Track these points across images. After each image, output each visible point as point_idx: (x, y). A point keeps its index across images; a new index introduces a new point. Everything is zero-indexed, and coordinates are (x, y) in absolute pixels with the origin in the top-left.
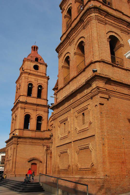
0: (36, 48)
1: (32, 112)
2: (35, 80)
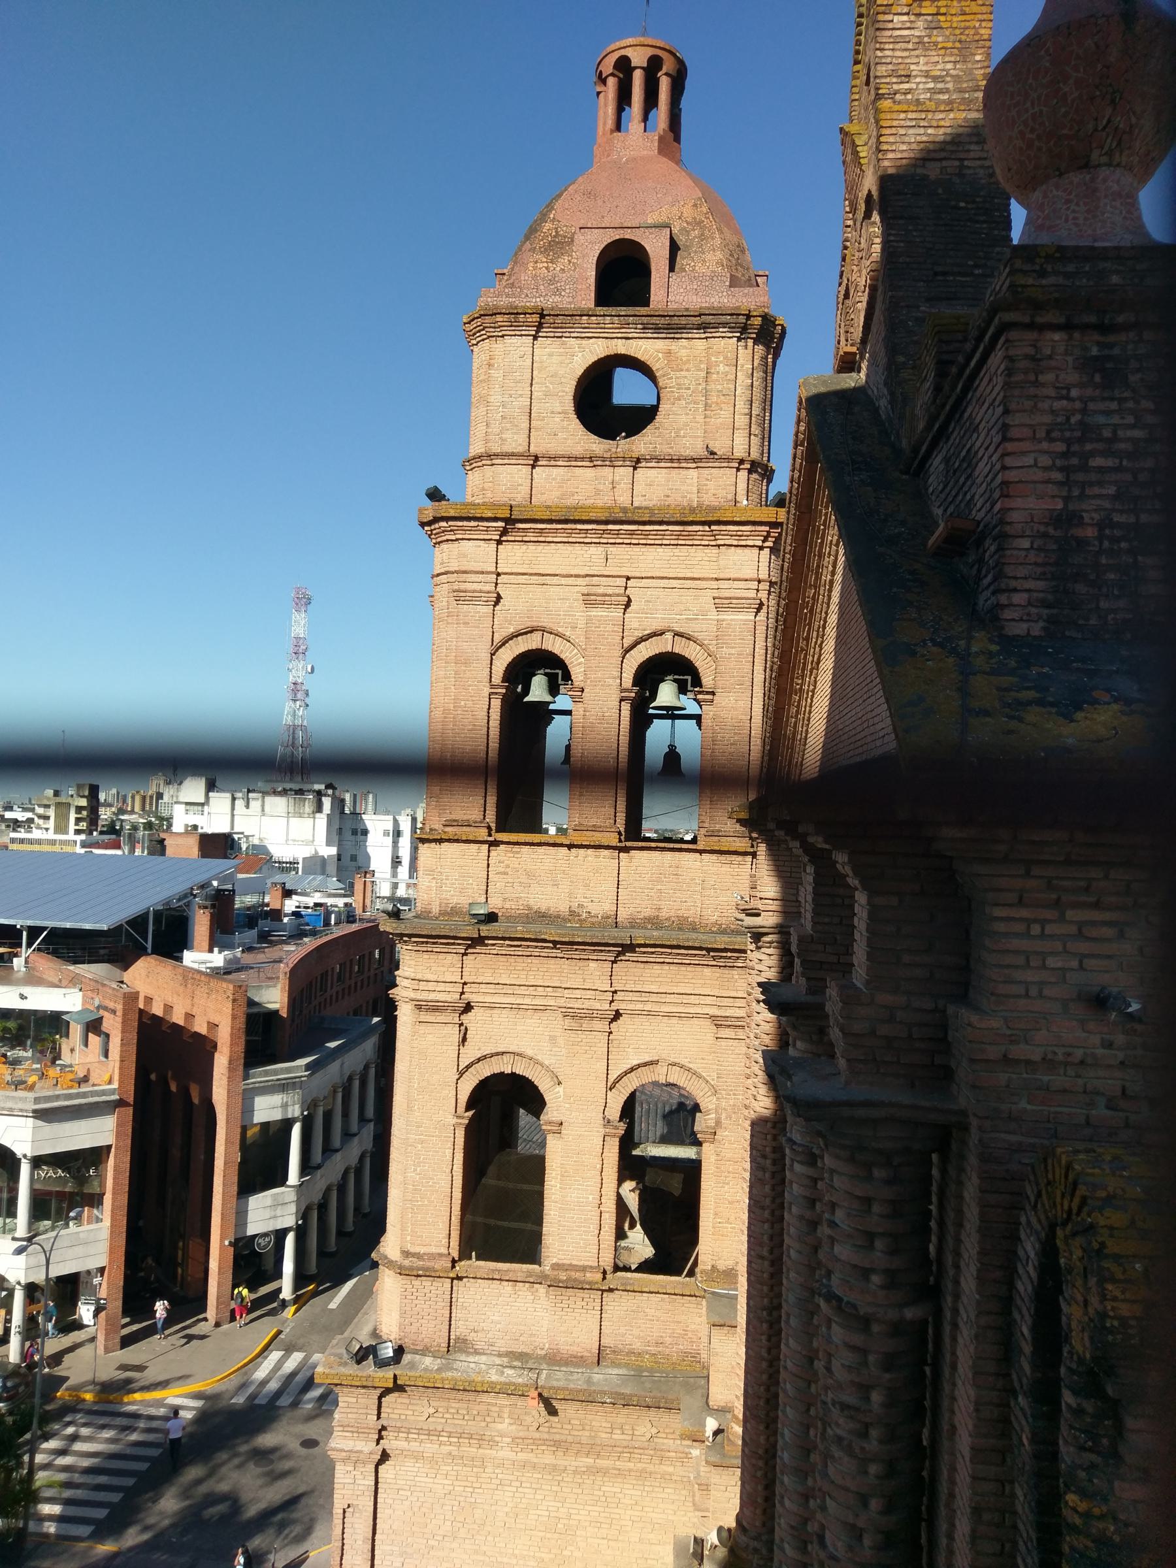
0: (638, 78)
1: (553, 1039)
2: (589, 600)
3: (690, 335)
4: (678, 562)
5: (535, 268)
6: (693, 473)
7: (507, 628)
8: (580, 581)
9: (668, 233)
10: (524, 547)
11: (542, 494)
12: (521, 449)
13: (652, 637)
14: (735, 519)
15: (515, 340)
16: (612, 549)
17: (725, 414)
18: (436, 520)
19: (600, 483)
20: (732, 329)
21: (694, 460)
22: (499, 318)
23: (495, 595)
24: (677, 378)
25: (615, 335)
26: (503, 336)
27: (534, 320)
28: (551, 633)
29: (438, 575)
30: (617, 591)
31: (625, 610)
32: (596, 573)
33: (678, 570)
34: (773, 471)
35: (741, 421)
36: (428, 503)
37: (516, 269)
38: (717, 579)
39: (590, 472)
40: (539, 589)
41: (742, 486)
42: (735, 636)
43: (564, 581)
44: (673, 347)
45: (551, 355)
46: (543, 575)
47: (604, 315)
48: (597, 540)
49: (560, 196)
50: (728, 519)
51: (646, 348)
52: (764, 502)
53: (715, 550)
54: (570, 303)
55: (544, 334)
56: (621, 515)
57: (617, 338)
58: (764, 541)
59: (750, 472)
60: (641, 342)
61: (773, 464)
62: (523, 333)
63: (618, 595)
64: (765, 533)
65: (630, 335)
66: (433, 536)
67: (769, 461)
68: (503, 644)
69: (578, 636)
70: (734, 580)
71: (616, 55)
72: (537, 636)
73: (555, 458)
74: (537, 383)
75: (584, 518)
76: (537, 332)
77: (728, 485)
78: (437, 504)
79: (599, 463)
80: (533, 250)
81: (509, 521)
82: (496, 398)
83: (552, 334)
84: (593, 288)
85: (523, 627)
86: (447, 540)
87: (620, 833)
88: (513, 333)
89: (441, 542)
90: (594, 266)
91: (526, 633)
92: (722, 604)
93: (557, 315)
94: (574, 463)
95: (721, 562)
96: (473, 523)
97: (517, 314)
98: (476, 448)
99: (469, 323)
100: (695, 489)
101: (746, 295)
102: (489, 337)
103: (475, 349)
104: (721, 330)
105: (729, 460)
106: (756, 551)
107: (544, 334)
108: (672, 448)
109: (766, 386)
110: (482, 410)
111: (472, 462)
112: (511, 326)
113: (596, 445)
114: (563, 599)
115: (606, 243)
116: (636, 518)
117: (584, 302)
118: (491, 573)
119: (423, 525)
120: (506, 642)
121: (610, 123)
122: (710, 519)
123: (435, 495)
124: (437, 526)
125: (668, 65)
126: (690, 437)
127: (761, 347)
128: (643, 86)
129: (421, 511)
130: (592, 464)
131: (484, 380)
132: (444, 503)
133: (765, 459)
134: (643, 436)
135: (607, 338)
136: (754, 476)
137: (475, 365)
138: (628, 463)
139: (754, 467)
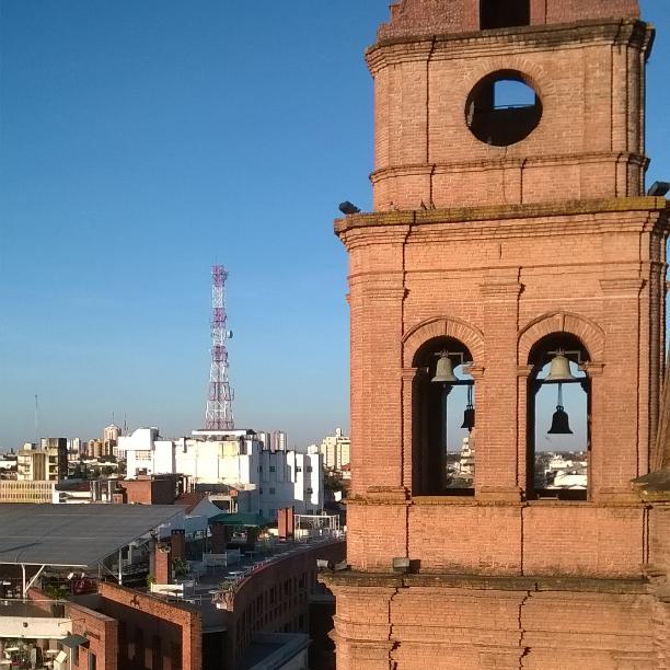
2: (485, 289)
8: (477, 274)
12: (419, 161)
15: (411, 65)
17: (603, 115)
20: (606, 36)
21: (575, 157)
22: (396, 47)
30: (510, 281)
34: (649, 161)
35: (619, 119)
36: (342, 215)
39: (482, 177)
40: (442, 283)
41: (621, 179)
47: (490, 36)
51: (528, 59)
53: (599, 239)
54: (458, 28)
60: (523, 57)
61: (648, 155)
63: (512, 284)
73: (451, 166)
76: (430, 56)
82: (396, 118)
83: (443, 57)
87: (522, 493)
92: (607, 285)
96: (381, 229)
98: (383, 163)
105: (609, 155)
113: (486, 150)
118: (399, 272)
119: (338, 233)
129: (337, 221)
131: (386, 103)
132: (356, 214)
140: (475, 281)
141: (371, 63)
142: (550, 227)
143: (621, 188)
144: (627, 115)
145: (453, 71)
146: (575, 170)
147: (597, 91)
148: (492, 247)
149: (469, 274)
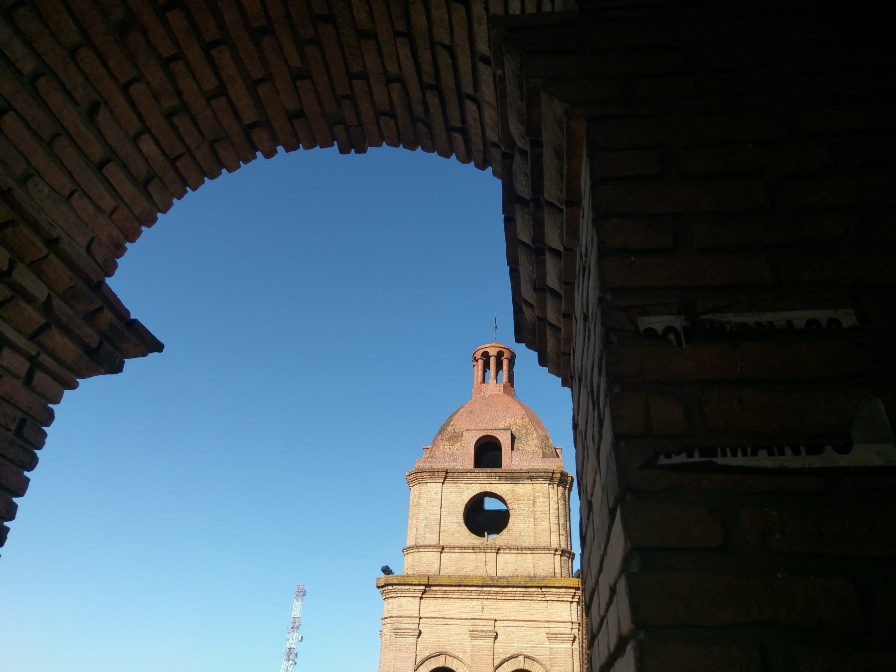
0: (493, 361)
2: (474, 634)
3: (524, 482)
4: (524, 610)
5: (443, 448)
6: (530, 556)
7: (425, 653)
8: (468, 622)
9: (510, 432)
10: (436, 601)
11: (446, 568)
12: (435, 543)
13: (511, 659)
14: (555, 585)
16: (486, 602)
17: (545, 524)
18: (386, 585)
19: (478, 562)
20: (545, 479)
22: (425, 474)
23: (418, 631)
24: (518, 504)
25: (484, 482)
26: (427, 483)
27: (443, 475)
28: (451, 656)
29: (385, 618)
31: (495, 641)
32: (477, 617)
33: (525, 615)
35: (554, 527)
36: (382, 575)
37: (434, 448)
38: (548, 622)
39: (473, 556)
40: (444, 627)
41: (558, 564)
42: (561, 658)
43: (458, 622)
44: (515, 488)
45: (451, 492)
46: (446, 619)
47: (479, 472)
48: (477, 597)
49: (456, 413)
50: (551, 585)
51: (501, 488)
52: (571, 575)
53: (545, 603)
54: (461, 466)
55: (448, 482)
56: (490, 582)
57: (485, 483)
58: (573, 598)
59: (561, 556)
60: (498, 486)
61: (574, 551)
62: (437, 481)
63: (490, 631)
64: (573, 594)
65: (492, 482)
66: (384, 594)
67: (571, 549)
68: (422, 664)
69: (467, 658)
70: (558, 622)
71: (482, 351)
72: (442, 657)
73: (453, 548)
74: (444, 507)
75: (469, 584)
76: (444, 481)
77: (551, 564)
78: (387, 576)
79: (478, 551)
80: (443, 440)
81: (427, 586)
82: (422, 515)
83: (452, 482)
84: (473, 458)
85: (434, 652)
86: (392, 597)
88: (432, 481)
89: (389, 598)
90: (473, 448)
91: (436, 656)
92: (552, 637)
93: (455, 472)
94: (463, 551)
95: (549, 611)
96: (407, 587)
97: (434, 472)
98: (410, 542)
99: (409, 476)
100: (531, 566)
101: (551, 462)
102: (419, 483)
103: (412, 488)
104: (539, 480)
105: (549, 549)
106: (569, 604)
107: (448, 482)
108: (517, 542)
109: (566, 508)
110: (414, 521)
111: (407, 550)
112: (431, 478)
113: (475, 540)
114: (458, 634)
115: (479, 437)
116: (499, 584)
117: (468, 466)
118: (416, 617)
119: (379, 587)
120: (424, 662)
121: (480, 379)
122: (541, 585)
123: (387, 571)
124: (386, 588)
125: (507, 354)
126: (527, 536)
127: (561, 487)
128: (495, 364)
129: (378, 579)
130: (473, 551)
132: (391, 575)
133: (569, 548)
134: (502, 535)
135: (480, 483)
136: (564, 558)
137: (411, 497)
138: (493, 551)
139: (563, 552)
140: (466, 627)
141: (410, 482)
142: (515, 593)
143: (558, 571)
144: (559, 525)
145: (457, 490)
146: (529, 557)
147: (541, 509)
148: (477, 604)
149: (462, 622)
